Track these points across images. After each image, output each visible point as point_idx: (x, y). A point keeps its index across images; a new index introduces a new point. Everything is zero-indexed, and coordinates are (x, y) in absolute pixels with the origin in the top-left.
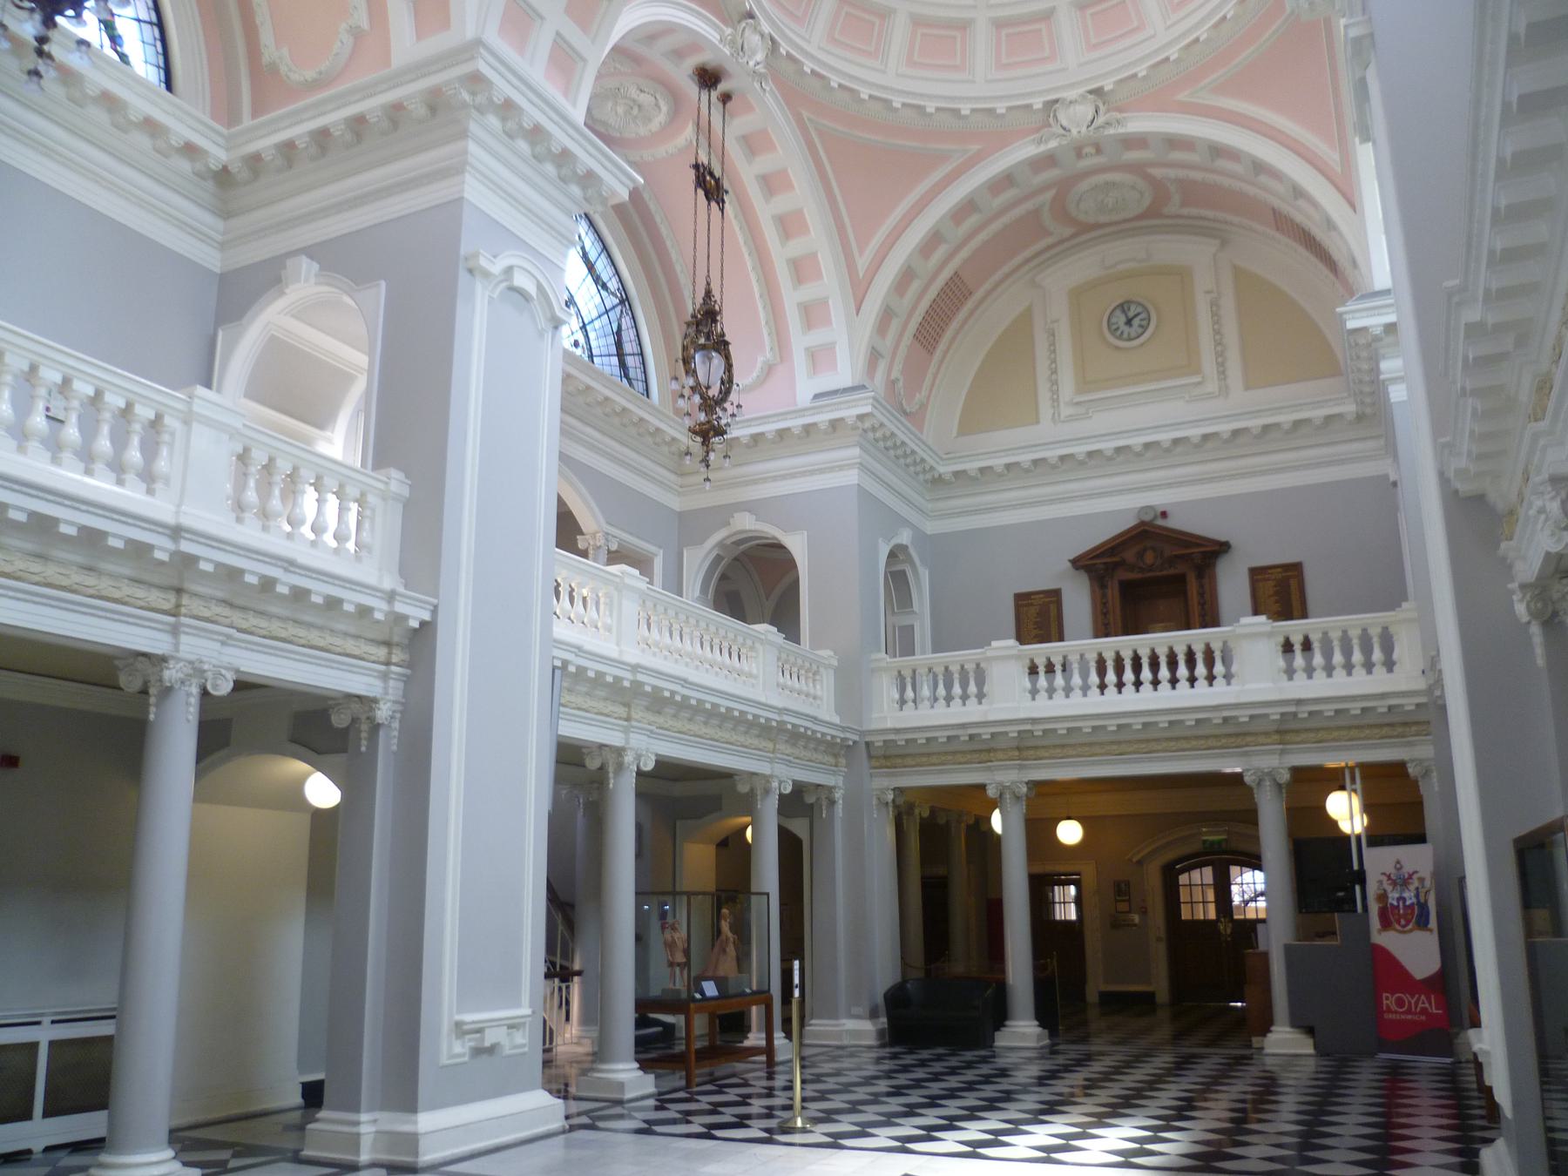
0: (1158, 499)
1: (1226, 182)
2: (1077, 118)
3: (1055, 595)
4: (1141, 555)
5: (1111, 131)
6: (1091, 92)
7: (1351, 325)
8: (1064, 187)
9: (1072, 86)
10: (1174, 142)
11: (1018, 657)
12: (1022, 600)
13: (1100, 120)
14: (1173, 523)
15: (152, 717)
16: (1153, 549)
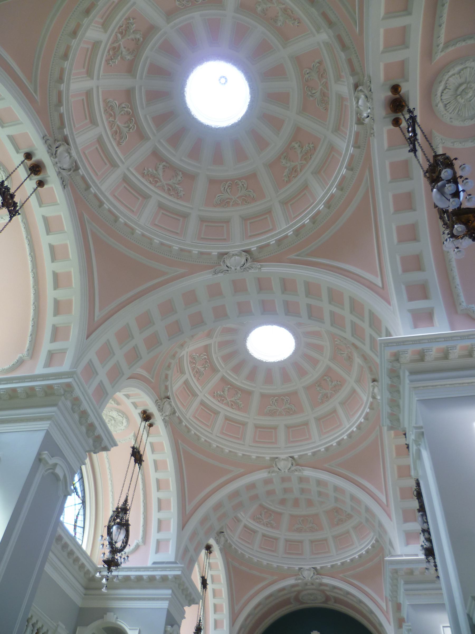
2: (308, 575)
5: (318, 581)
8: (299, 592)
10: (335, 587)
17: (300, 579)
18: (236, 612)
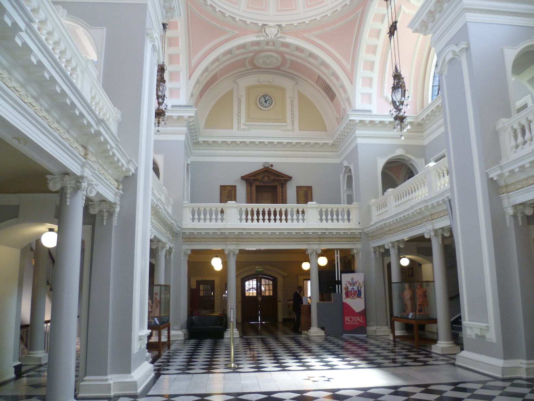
0: (271, 160)
1: (308, 65)
2: (272, 32)
3: (235, 187)
4: (263, 178)
5: (281, 40)
6: (277, 25)
7: (351, 118)
8: (257, 52)
9: (272, 21)
10: (298, 49)
11: (236, 207)
12: (223, 188)
13: (278, 35)
14: (274, 168)
15: (68, 203)
16: (268, 176)
17: (263, 36)
18: (192, 66)
